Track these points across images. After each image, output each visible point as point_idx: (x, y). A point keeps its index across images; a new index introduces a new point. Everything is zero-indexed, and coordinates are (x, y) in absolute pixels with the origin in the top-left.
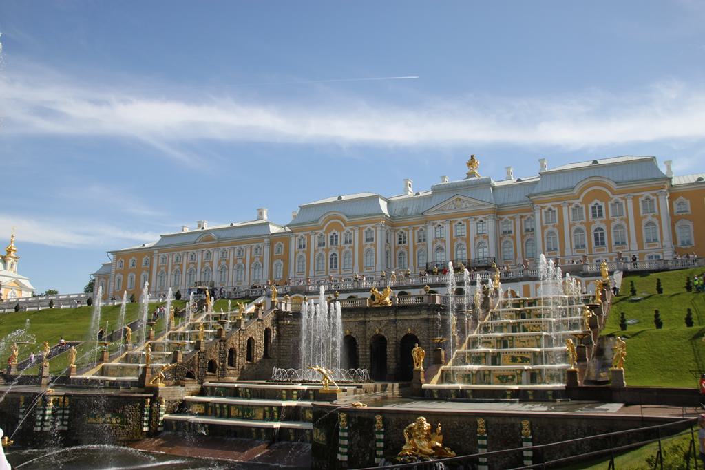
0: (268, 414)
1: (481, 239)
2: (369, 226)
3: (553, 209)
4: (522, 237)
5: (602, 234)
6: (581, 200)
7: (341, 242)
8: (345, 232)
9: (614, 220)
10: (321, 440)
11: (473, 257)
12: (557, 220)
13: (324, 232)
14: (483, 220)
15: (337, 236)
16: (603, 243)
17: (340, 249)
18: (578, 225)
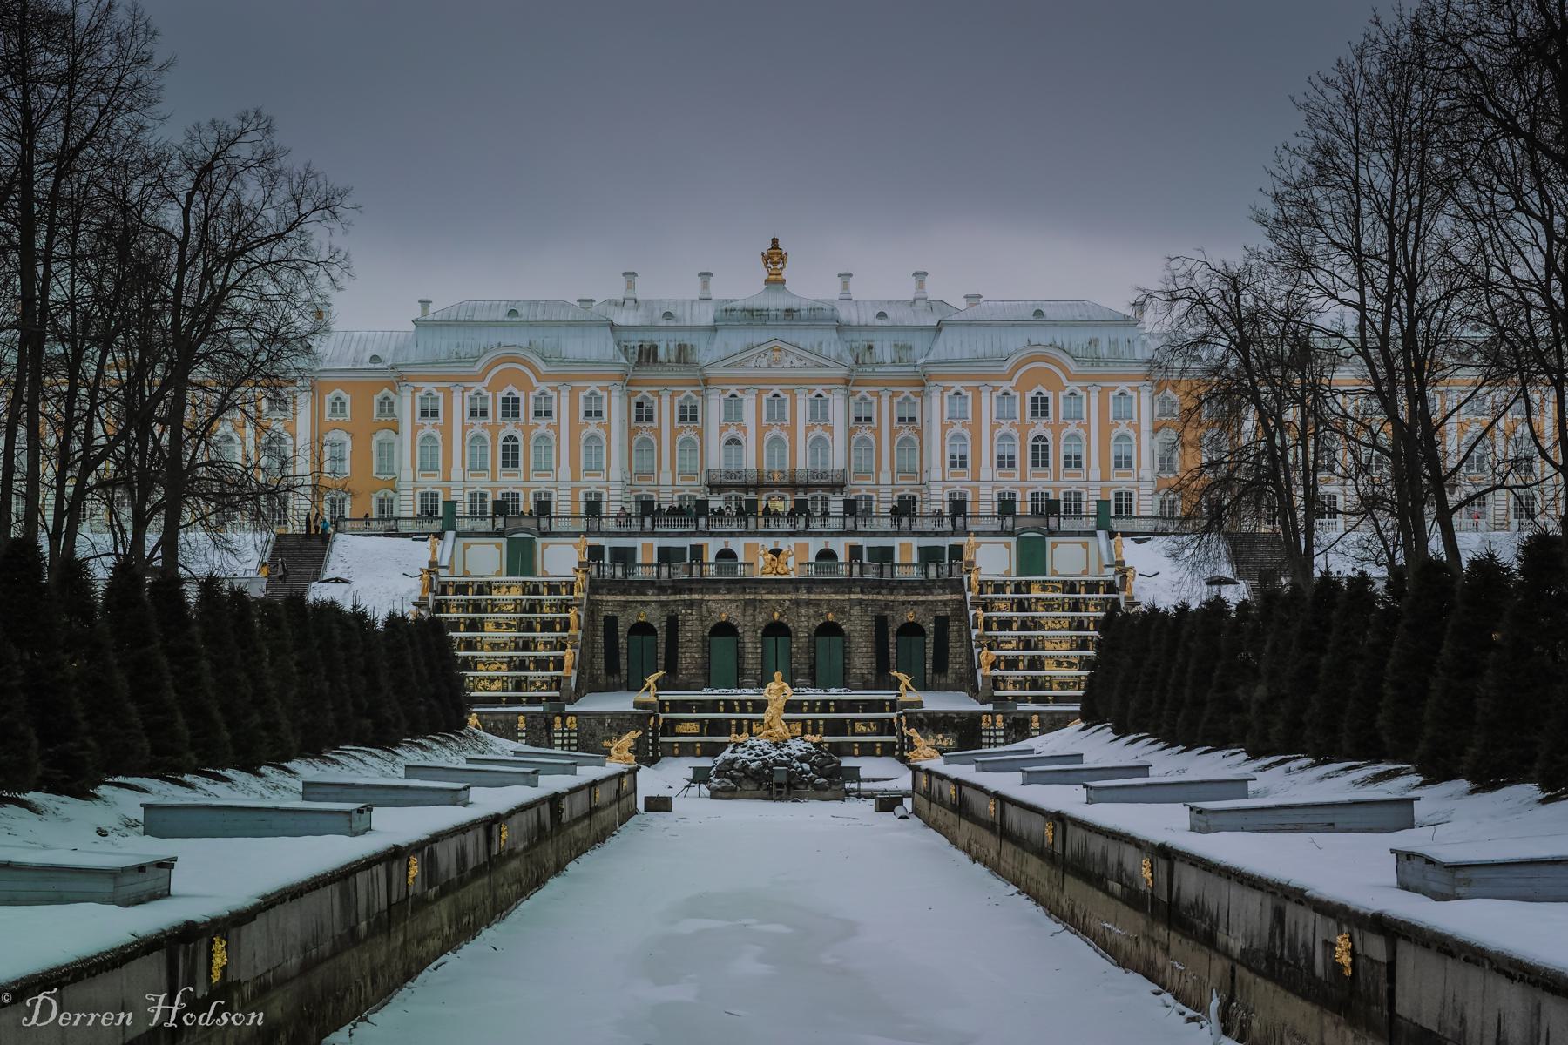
0: (809, 729)
1: (818, 431)
2: (593, 386)
3: (964, 393)
4: (893, 433)
5: (1045, 448)
6: (1013, 383)
7: (527, 408)
8: (536, 393)
9: (1067, 425)
10: (945, 744)
11: (801, 465)
12: (970, 416)
13: (488, 389)
14: (825, 395)
15: (516, 400)
16: (1045, 464)
17: (527, 430)
18: (1005, 429)
